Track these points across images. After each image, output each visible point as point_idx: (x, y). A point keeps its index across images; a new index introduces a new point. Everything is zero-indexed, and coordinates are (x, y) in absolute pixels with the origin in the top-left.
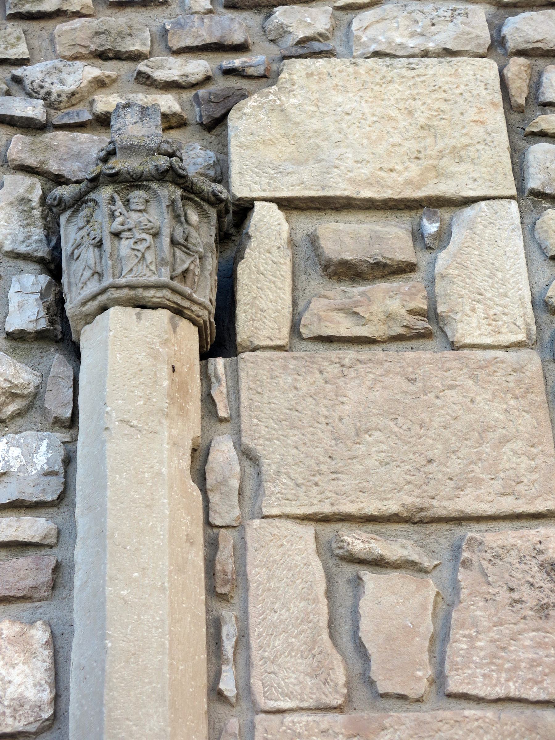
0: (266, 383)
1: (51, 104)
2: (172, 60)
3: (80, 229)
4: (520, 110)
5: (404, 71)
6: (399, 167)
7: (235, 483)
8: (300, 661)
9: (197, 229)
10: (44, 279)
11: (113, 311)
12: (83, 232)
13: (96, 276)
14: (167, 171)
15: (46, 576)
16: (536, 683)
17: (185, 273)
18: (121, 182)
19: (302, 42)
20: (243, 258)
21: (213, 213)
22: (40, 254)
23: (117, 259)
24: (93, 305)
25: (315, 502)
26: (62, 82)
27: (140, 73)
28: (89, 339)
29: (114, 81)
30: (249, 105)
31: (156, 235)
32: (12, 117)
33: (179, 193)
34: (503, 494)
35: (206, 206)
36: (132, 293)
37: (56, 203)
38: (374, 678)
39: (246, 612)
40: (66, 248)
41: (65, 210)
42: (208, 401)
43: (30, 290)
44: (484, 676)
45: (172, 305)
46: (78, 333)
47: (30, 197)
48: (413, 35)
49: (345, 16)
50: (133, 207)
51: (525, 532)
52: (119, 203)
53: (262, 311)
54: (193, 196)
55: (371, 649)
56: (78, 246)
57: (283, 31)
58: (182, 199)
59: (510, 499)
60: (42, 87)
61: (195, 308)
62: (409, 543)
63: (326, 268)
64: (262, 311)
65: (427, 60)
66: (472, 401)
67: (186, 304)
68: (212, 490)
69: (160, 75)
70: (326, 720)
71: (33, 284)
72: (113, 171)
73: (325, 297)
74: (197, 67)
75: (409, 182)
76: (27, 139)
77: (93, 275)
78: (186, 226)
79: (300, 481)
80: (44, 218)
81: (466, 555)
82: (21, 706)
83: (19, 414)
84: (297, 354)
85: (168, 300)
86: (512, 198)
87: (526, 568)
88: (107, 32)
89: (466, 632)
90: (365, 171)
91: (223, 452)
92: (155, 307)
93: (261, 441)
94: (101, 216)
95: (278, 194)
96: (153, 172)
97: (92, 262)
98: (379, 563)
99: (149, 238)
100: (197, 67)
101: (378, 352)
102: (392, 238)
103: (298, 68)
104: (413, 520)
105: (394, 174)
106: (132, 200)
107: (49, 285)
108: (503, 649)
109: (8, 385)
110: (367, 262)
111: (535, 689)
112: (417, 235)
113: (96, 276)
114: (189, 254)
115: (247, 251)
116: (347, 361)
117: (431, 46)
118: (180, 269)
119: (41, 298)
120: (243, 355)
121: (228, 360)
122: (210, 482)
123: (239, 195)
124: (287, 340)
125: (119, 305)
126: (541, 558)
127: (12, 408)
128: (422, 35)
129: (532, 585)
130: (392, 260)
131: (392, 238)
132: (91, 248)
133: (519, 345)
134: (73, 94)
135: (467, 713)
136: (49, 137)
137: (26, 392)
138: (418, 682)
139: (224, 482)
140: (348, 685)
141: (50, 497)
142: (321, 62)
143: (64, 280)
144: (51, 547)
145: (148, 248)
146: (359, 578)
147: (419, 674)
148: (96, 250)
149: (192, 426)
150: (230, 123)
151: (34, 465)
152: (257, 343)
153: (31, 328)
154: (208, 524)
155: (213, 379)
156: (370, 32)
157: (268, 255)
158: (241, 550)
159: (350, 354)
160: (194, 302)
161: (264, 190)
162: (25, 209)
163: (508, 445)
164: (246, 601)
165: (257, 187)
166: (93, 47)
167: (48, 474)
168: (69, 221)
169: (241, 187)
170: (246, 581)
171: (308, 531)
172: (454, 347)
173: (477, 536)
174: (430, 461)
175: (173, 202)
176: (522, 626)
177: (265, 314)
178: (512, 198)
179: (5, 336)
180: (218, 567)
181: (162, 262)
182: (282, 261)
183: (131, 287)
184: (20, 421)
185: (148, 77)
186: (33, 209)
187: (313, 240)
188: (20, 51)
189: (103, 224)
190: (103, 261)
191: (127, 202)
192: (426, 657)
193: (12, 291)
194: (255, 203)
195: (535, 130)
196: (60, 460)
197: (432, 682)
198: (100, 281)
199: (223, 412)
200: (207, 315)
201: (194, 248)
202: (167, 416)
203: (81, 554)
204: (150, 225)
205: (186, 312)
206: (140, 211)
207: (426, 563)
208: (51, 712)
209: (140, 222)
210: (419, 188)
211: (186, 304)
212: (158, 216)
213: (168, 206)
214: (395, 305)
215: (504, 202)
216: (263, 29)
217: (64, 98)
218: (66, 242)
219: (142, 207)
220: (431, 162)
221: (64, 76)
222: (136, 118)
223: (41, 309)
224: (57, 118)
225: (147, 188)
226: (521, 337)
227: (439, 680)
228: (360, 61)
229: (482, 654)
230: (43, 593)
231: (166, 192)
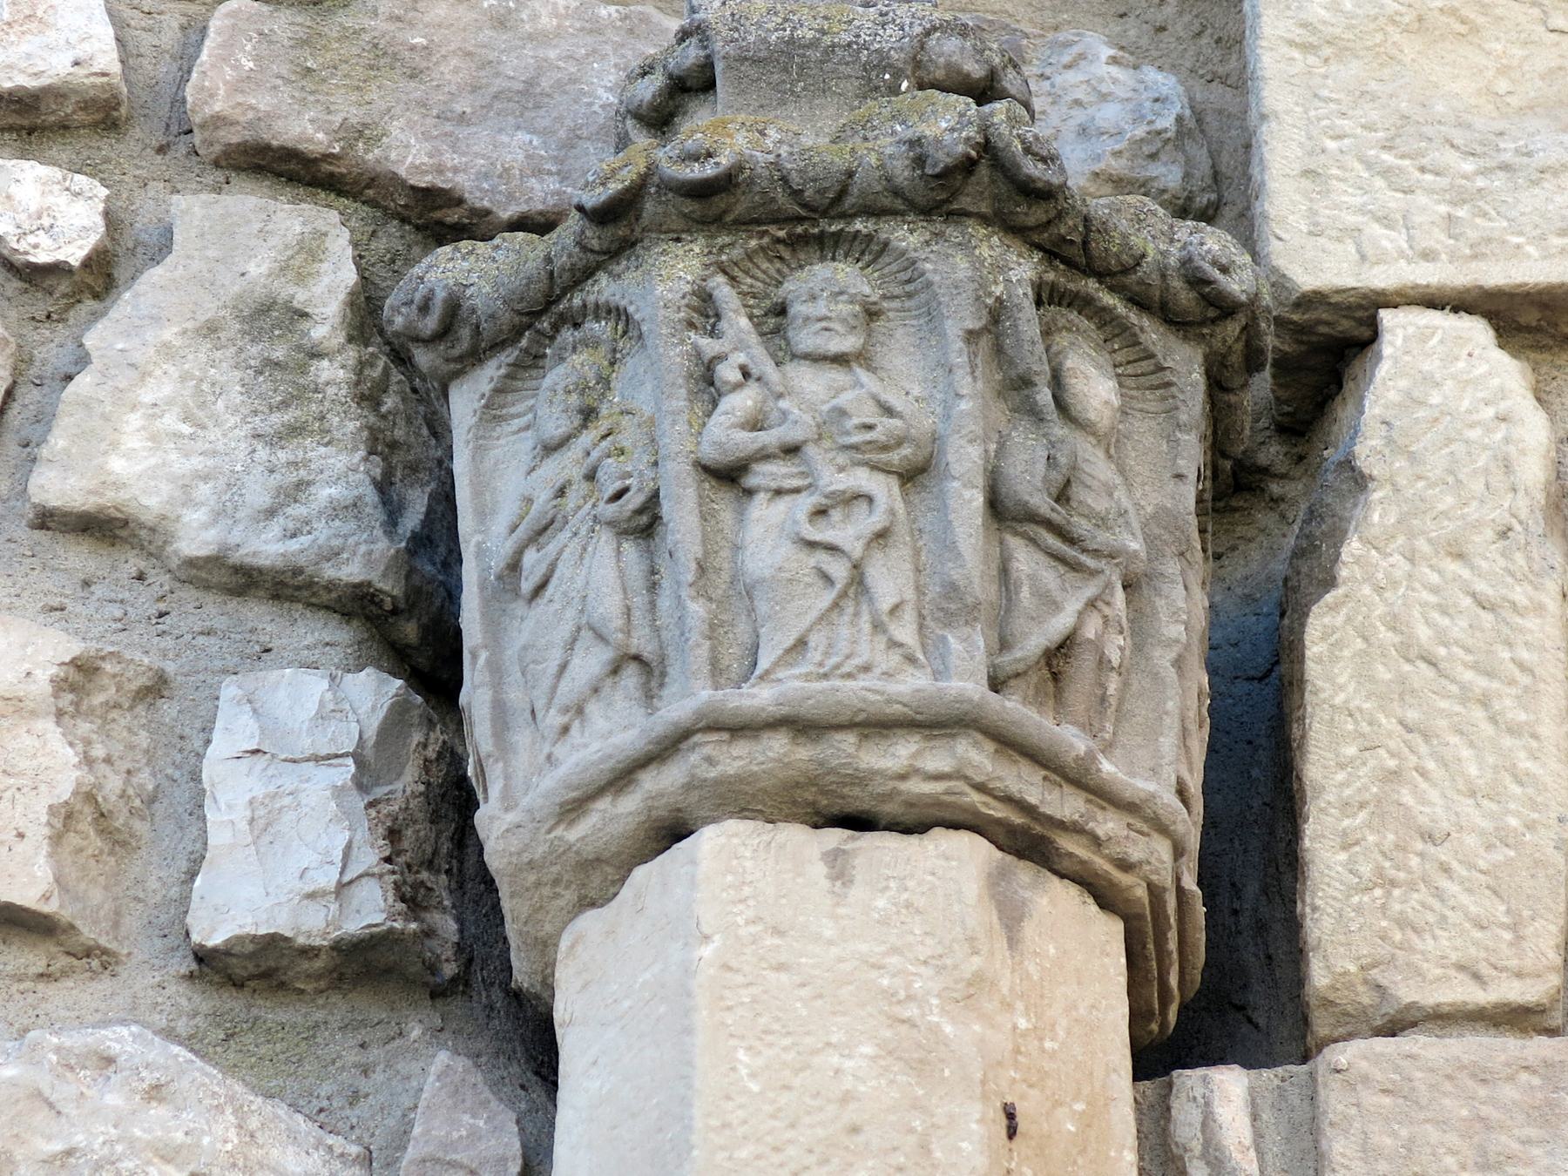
3: (550, 448)
9: (1112, 443)
10: (373, 693)
11: (713, 843)
12: (567, 465)
13: (631, 677)
14: (967, 166)
17: (1060, 653)
18: (746, 223)
20: (1330, 582)
21: (1186, 365)
22: (351, 571)
24: (621, 814)
28: (597, 979)
31: (913, 475)
33: (1024, 269)
35: (1152, 333)
36: (804, 754)
37: (430, 324)
40: (483, 541)
41: (475, 357)
43: (305, 745)
45: (998, 811)
46: (546, 947)
47: (300, 297)
50: (806, 339)
52: (737, 323)
53: (1429, 837)
54: (1091, 285)
56: (541, 533)
58: (1039, 303)
61: (1109, 825)
64: (1429, 837)
67: (1066, 805)
71: (321, 716)
72: (708, 170)
77: (615, 671)
78: (1059, 430)
80: (369, 398)
85: (981, 788)
94: (650, 385)
95: (1496, 275)
96: (902, 171)
97: (608, 607)
99: (884, 489)
106: (798, 309)
107: (396, 720)
113: (631, 677)
114: (1074, 567)
115: (1352, 547)
118: (1034, 641)
119: (361, 785)
120: (1343, 1054)
121: (1268, 1076)
123: (1306, 279)
124: (1555, 980)
125: (744, 812)
132: (605, 541)
143: (475, 694)
145: (882, 536)
148: (630, 548)
152: (1408, 993)
153: (313, 925)
157: (1453, 567)
160: (1104, 796)
161: (1428, 256)
162: (279, 354)
165: (1390, 240)
168: (492, 412)
169: (1313, 243)
177: (1443, 854)
181: (949, 606)
182: (1519, 594)
183: (801, 726)
186: (315, 354)
189: (660, 423)
190: (665, 603)
191: (774, 319)
193: (221, 746)
194: (1386, 316)
198: (649, 697)
200: (1163, 860)
201: (1102, 538)
204: (886, 427)
206: (840, 360)
209: (842, 413)
211: (1066, 805)
212: (922, 381)
213: (971, 336)
218: (482, 515)
219: (847, 343)
223: (362, 834)
225: (870, 251)
231: (962, 266)
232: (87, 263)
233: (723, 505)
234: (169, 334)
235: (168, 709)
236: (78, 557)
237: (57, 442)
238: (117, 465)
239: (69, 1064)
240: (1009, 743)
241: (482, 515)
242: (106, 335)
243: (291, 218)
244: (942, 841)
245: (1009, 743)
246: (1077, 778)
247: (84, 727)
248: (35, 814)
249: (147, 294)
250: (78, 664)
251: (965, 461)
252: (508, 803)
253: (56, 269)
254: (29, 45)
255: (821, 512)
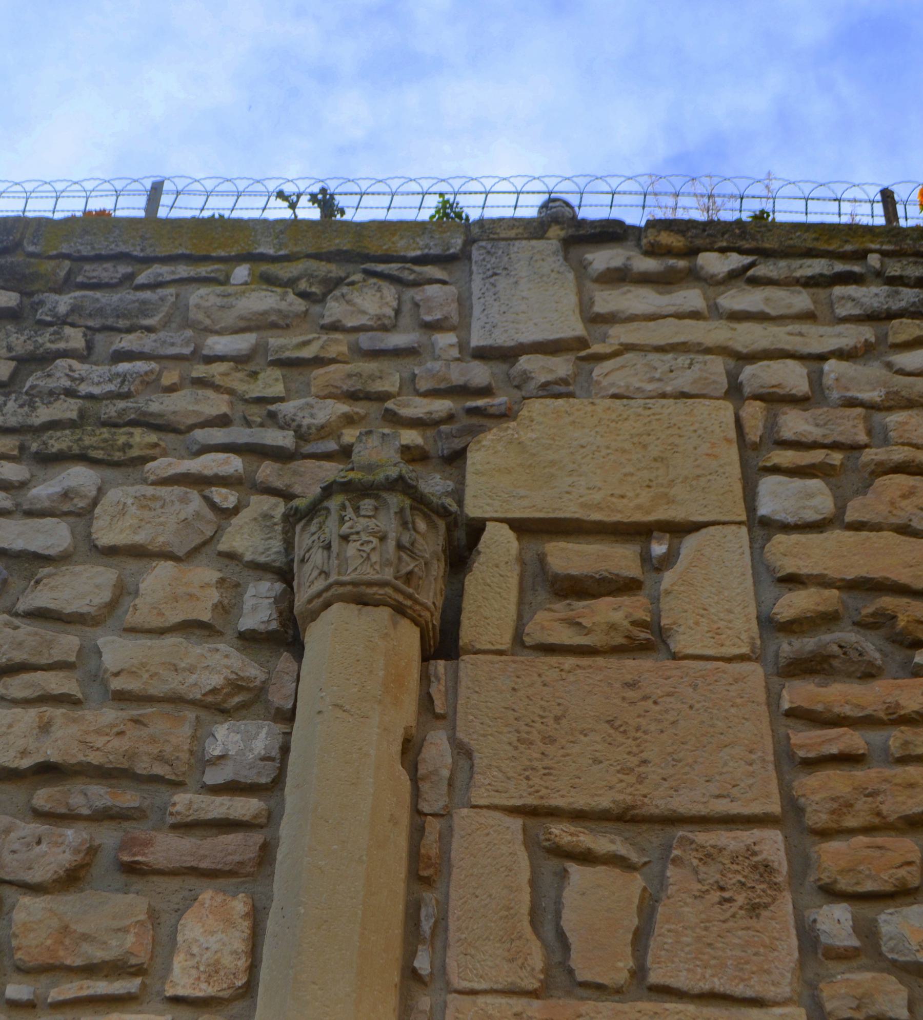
0: (485, 689)
1: (301, 436)
2: (418, 399)
3: (313, 534)
4: (756, 447)
5: (640, 410)
6: (629, 494)
7: (446, 773)
8: (498, 945)
9: (423, 536)
10: (279, 587)
11: (335, 606)
12: (315, 537)
13: (323, 576)
15: (252, 853)
16: (742, 980)
17: (410, 573)
19: (544, 386)
20: (471, 571)
21: (442, 524)
22: (277, 564)
23: (343, 561)
25: (525, 794)
26: (312, 416)
27: (387, 410)
28: (316, 637)
29: (363, 418)
30: (488, 438)
31: (383, 539)
32: (264, 446)
33: (408, 502)
34: (718, 797)
35: (435, 517)
37: (292, 512)
38: (573, 966)
39: (447, 896)
40: (298, 553)
41: (300, 520)
42: (426, 701)
43: (264, 595)
44: (688, 970)
45: (393, 602)
47: (273, 513)
48: (652, 380)
49: (586, 366)
50: (363, 513)
51: (739, 833)
52: (350, 510)
53: (486, 618)
54: (422, 507)
55: (572, 939)
56: (308, 551)
57: (526, 377)
58: (411, 509)
59: (724, 801)
60: (293, 420)
61: (418, 607)
62: (618, 839)
63: (553, 584)
64: (486, 618)
65: (664, 401)
66: (691, 707)
67: (409, 603)
68: (422, 779)
69: (406, 412)
70: (518, 1004)
71: (269, 590)
72: (345, 480)
73: (550, 610)
74: (442, 406)
75: (639, 507)
76: (277, 466)
77: (320, 574)
78: (413, 532)
79: (511, 774)
81: (676, 852)
82: (217, 972)
83: (243, 706)
84: (518, 658)
85: (390, 597)
86: (740, 523)
87: (739, 868)
88: (359, 375)
89: (673, 927)
90: (597, 497)
91: (437, 751)
92: (376, 605)
93: (475, 736)
94: (332, 524)
95: (510, 515)
96: (383, 480)
98: (587, 858)
99: (375, 541)
100: (442, 406)
101: (600, 661)
102: (622, 559)
103: (537, 408)
104: (624, 818)
105: (625, 501)
106: (362, 507)
107: (284, 590)
108: (710, 945)
109: (234, 676)
110: (592, 577)
111: (741, 987)
112: (646, 558)
113: (323, 576)
114: (414, 558)
115: (476, 565)
116: (566, 667)
117: (669, 389)
118: (404, 570)
119: (275, 602)
120: (465, 657)
122: (422, 771)
123: (471, 515)
124: (509, 645)
125: (342, 601)
126: (755, 859)
127: (237, 699)
128: (660, 380)
129: (743, 884)
130: (617, 575)
131: (622, 559)
132: (320, 550)
133: (742, 658)
134: (322, 427)
135: (667, 1005)
136: (295, 465)
137: (252, 685)
138: (618, 971)
139: (435, 772)
140: (546, 970)
141: (263, 780)
142: (560, 401)
143: (295, 583)
144: (262, 827)
145: (374, 549)
146: (566, 870)
147: (621, 964)
148: (325, 552)
149: (406, 713)
150: (469, 455)
151: (251, 750)
152: (478, 646)
153: (262, 628)
154: (417, 812)
155: (433, 679)
156: (610, 379)
157: (496, 569)
158: (446, 837)
159: (569, 662)
160: (416, 601)
161: (496, 511)
162: (268, 524)
163: (727, 750)
164: (448, 887)
165: (488, 508)
166: (345, 388)
167: (263, 759)
168: (303, 529)
169: (473, 509)
170: (450, 866)
171: (516, 823)
172: (675, 657)
173: (690, 835)
174: (644, 762)
175: (401, 511)
176: (730, 924)
177: (488, 621)
178: (740, 523)
179: (236, 635)
180: (423, 851)
181: (388, 563)
182: (509, 574)
183: (355, 584)
184: (244, 712)
185: (395, 414)
186: (275, 524)
187: (542, 559)
188: (278, 389)
189: (332, 528)
190: (331, 561)
191: (357, 509)
192: (629, 950)
194: (487, 523)
195: (769, 464)
196: (277, 747)
197: (633, 973)
199: (439, 708)
201: (420, 554)
202: (380, 702)
203: (285, 830)
205: (409, 611)
206: (369, 517)
207: (634, 857)
208: (244, 981)
209: (368, 526)
210: (648, 513)
211: (409, 603)
212: (388, 523)
213: (396, 513)
214: (618, 617)
215: (733, 527)
216: (508, 375)
217: (313, 430)
218: (300, 548)
219: (371, 513)
220: (662, 490)
221: (315, 411)
222: (376, 443)
223: (274, 611)
224: (308, 448)
225: (377, 497)
226: (745, 650)
227: (639, 973)
228: (597, 401)
229: (687, 949)
230: (249, 869)
231: (395, 500)
232: (234, 508)
233: (344, 544)
234: (247, 520)
235: (239, 589)
236: (226, 561)
237: (223, 539)
238: (234, 544)
239: (210, 650)
240: (397, 589)
241: (300, 548)
242: (235, 521)
243: (273, 500)
244: (381, 608)
245: (397, 589)
246: (410, 597)
247: (222, 590)
248: (209, 605)
249: (245, 515)
250: (221, 578)
251: (392, 536)
252: (299, 601)
253: (227, 509)
254: (226, 467)
255: (362, 544)
